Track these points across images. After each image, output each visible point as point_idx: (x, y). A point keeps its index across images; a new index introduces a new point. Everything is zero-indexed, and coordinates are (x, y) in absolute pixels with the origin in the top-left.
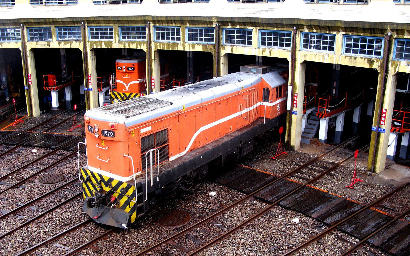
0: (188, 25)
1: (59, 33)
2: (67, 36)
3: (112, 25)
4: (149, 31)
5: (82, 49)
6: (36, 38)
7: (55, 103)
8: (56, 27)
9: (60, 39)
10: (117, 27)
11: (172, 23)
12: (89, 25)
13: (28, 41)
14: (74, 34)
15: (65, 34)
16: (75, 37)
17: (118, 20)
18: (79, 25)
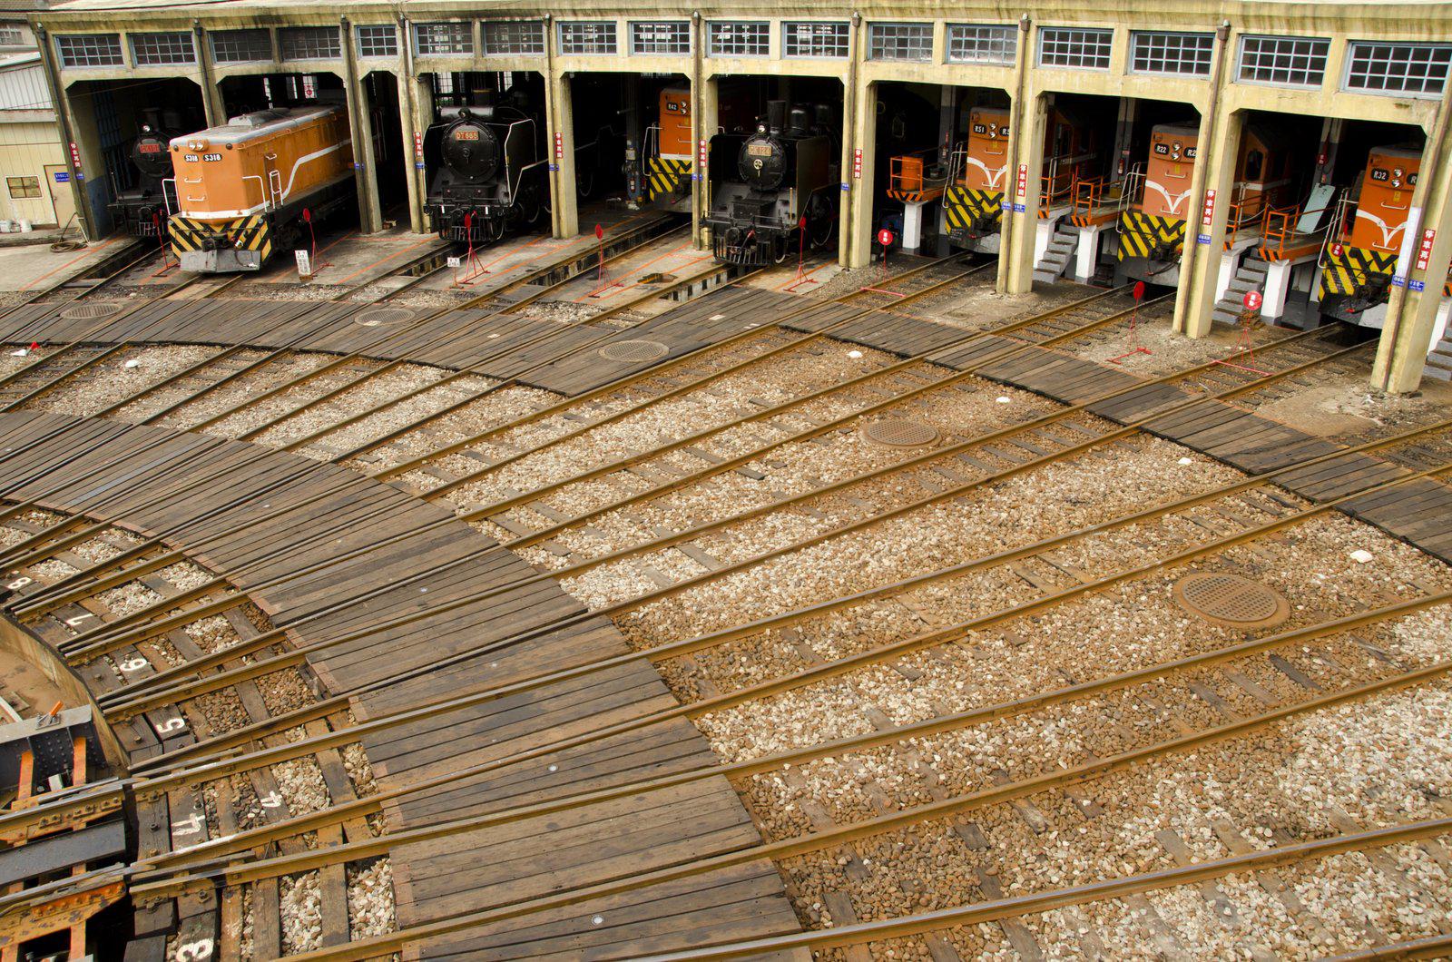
0: (1357, 35)
1: (954, 42)
2: (976, 50)
3: (1109, 26)
4: (1223, 49)
5: (1012, 94)
6: (890, 53)
7: (911, 237)
8: (947, 24)
9: (953, 59)
10: (1126, 34)
11: (1303, 27)
12: (1042, 23)
13: (867, 59)
14: (994, 45)
15: (970, 45)
16: (998, 56)
17: (1131, 12)
18: (1013, 22)
